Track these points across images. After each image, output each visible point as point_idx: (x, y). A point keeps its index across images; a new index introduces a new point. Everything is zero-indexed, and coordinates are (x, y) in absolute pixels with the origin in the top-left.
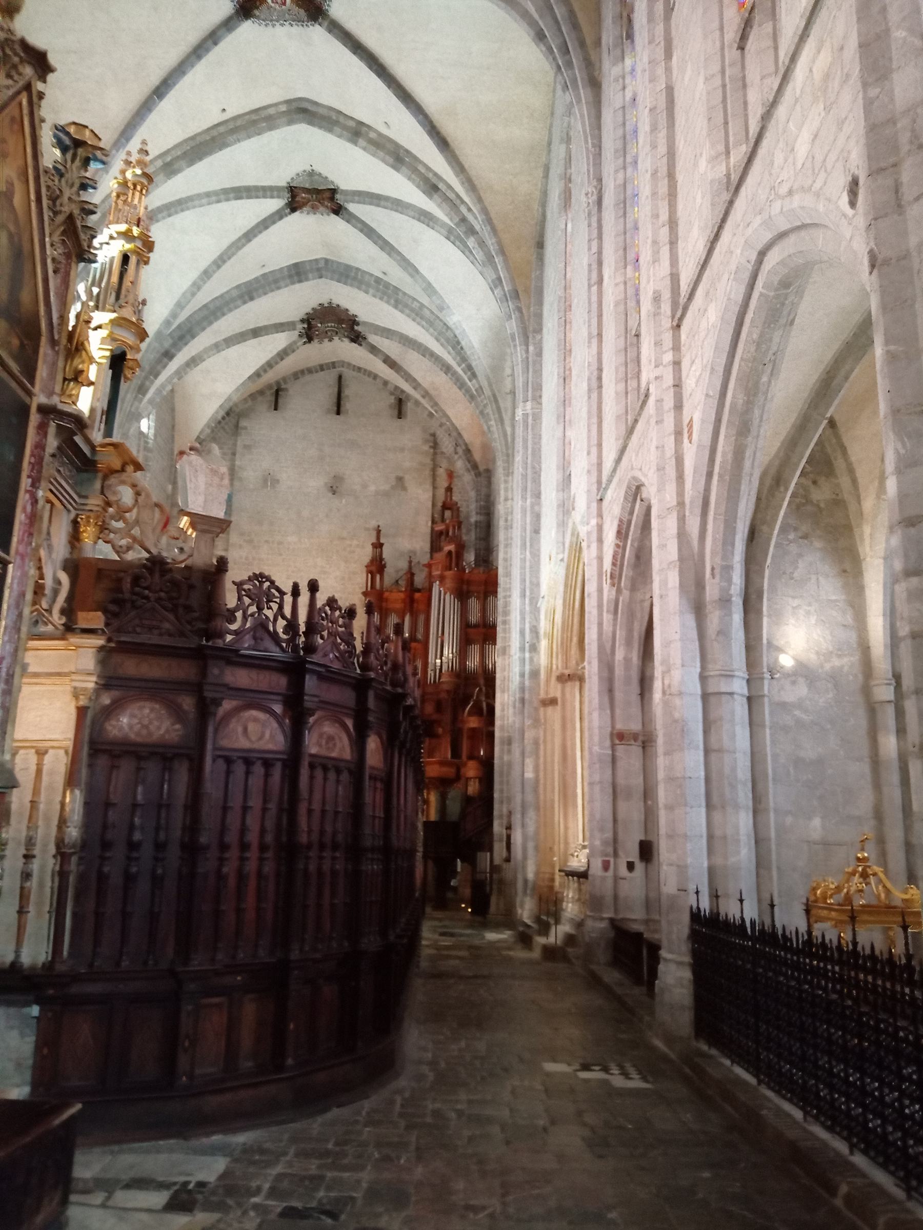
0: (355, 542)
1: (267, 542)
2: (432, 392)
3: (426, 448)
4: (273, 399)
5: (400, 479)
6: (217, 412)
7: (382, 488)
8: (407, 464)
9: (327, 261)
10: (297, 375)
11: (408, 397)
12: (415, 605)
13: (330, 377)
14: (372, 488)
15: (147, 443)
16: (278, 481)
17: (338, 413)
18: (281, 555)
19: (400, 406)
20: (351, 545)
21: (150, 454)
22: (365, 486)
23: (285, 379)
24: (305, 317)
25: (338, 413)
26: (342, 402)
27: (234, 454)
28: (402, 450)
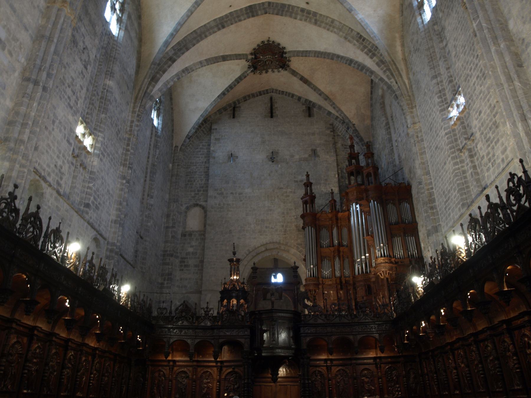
0: (289, 190)
1: (232, 193)
2: (331, 97)
3: (328, 132)
4: (232, 112)
5: (314, 152)
6: (199, 119)
7: (303, 156)
8: (318, 142)
9: (269, 3)
10: (246, 98)
11: (314, 105)
12: (339, 221)
13: (266, 98)
14: (297, 157)
15: (157, 132)
16: (237, 157)
17: (272, 117)
18: (241, 201)
19: (309, 109)
20: (286, 192)
21: (158, 139)
22: (292, 156)
23: (238, 100)
24: (253, 52)
25: (272, 117)
26: (274, 111)
27: (209, 145)
28: (313, 134)
